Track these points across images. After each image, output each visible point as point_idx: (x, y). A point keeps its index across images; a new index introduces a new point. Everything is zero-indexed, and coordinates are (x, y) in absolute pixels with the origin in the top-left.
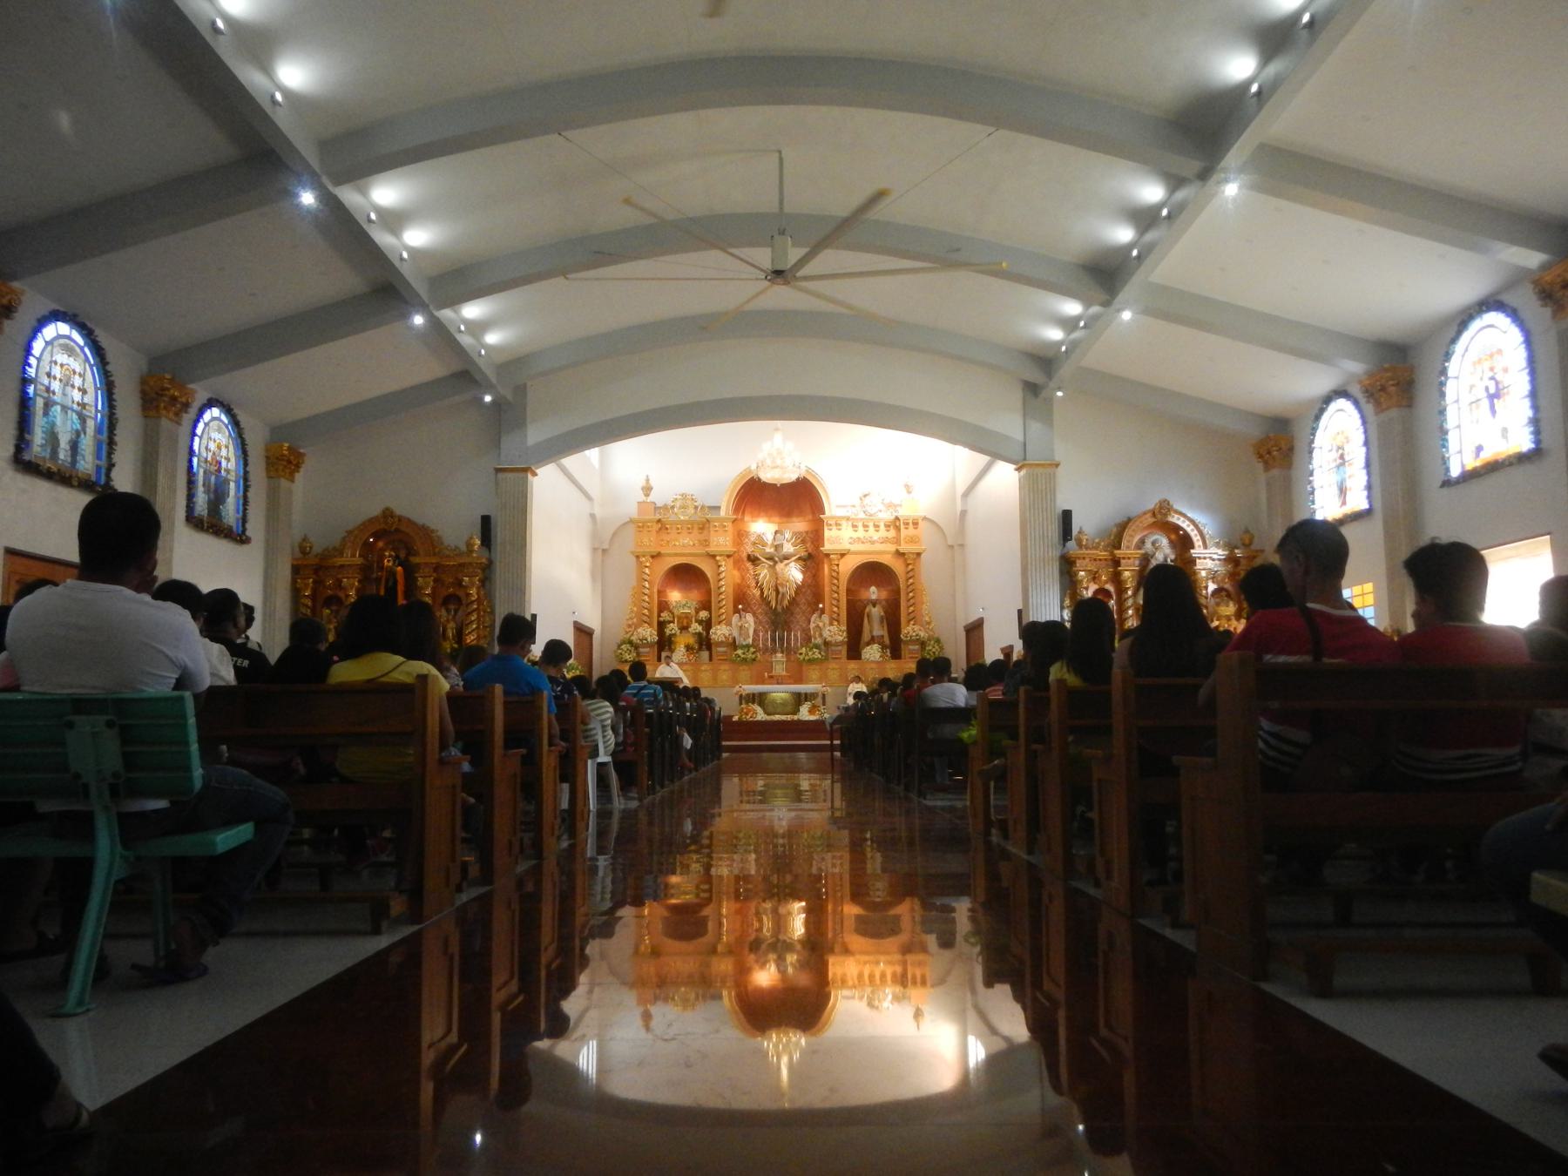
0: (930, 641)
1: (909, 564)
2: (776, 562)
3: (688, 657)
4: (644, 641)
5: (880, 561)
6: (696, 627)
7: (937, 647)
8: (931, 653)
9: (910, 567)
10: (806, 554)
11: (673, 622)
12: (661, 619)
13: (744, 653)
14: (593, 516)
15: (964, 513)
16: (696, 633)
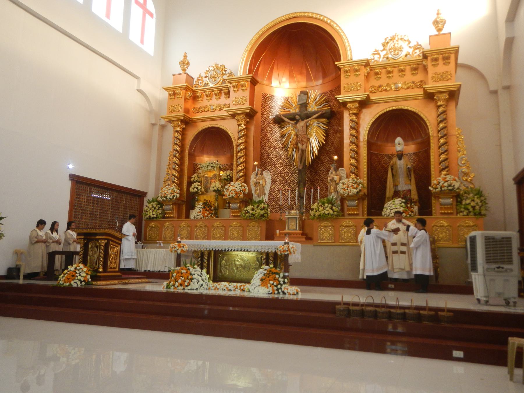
0: (469, 194)
1: (439, 107)
2: (297, 121)
3: (203, 213)
4: (164, 198)
5: (406, 108)
6: (217, 184)
7: (478, 201)
8: (470, 207)
9: (441, 110)
10: (329, 111)
11: (200, 182)
12: (192, 180)
13: (253, 210)
14: (139, 91)
15: (510, 42)
16: (214, 191)
